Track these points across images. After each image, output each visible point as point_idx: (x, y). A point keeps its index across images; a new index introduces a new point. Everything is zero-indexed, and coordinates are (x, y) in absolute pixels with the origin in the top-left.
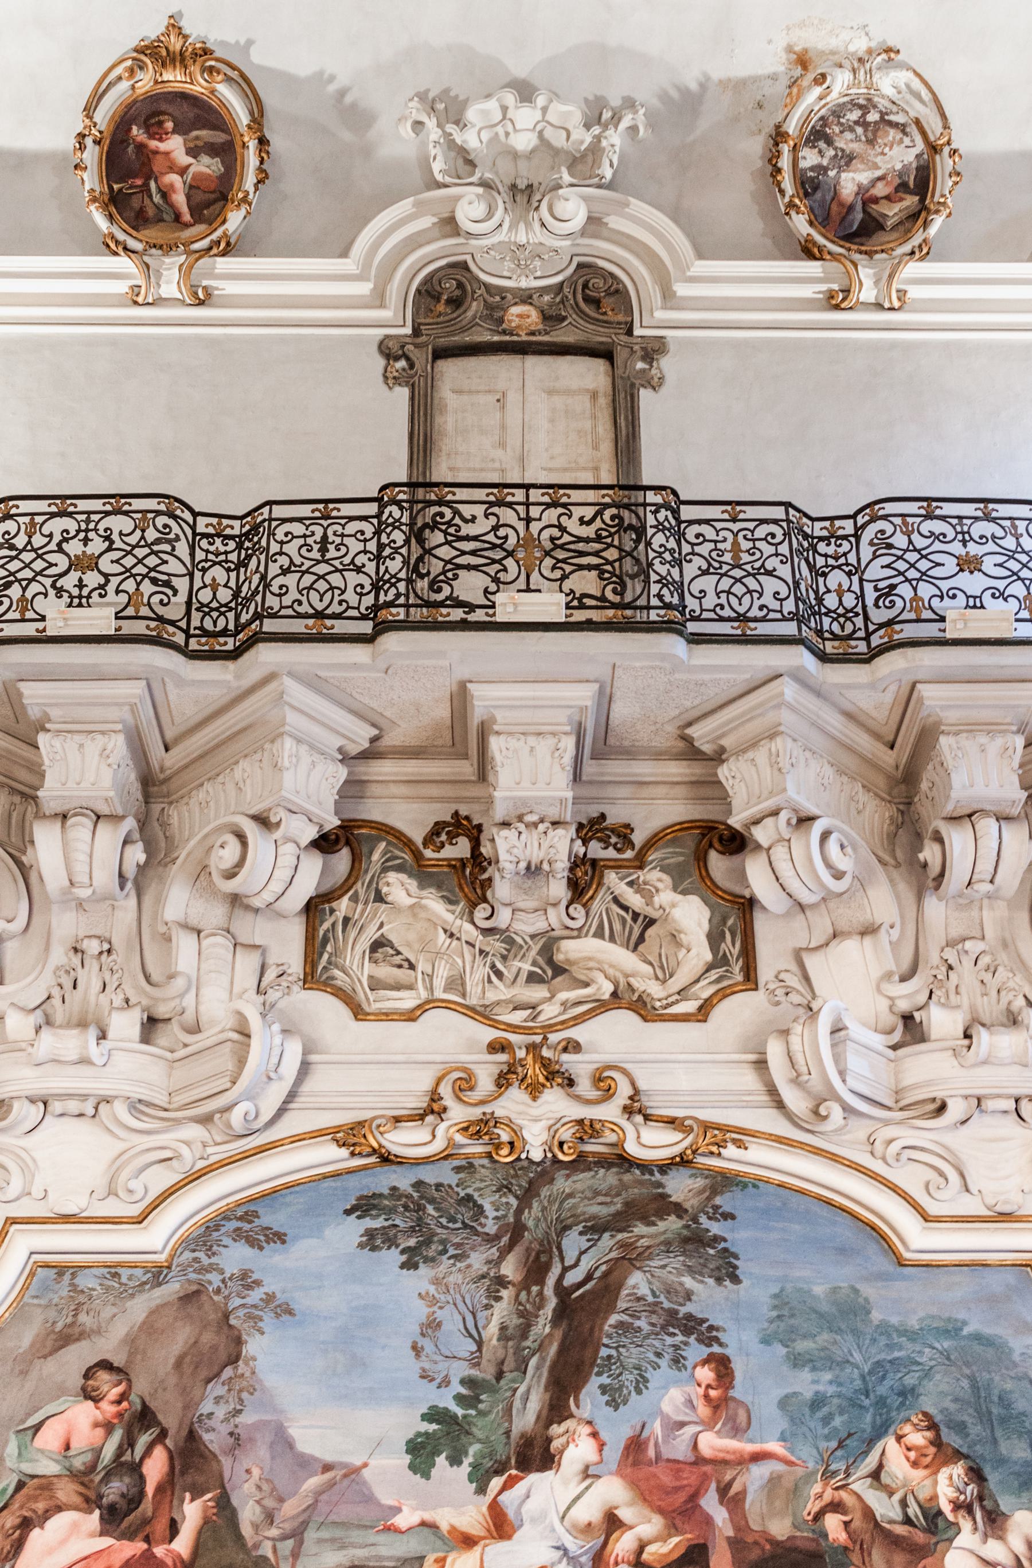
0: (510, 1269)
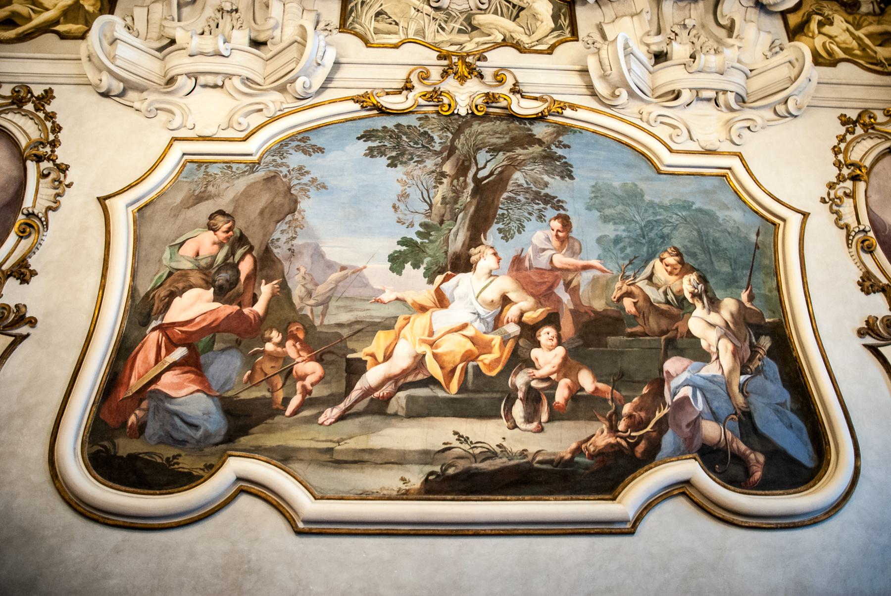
0: (448, 168)
